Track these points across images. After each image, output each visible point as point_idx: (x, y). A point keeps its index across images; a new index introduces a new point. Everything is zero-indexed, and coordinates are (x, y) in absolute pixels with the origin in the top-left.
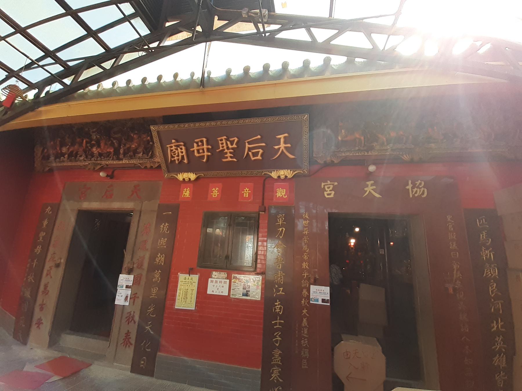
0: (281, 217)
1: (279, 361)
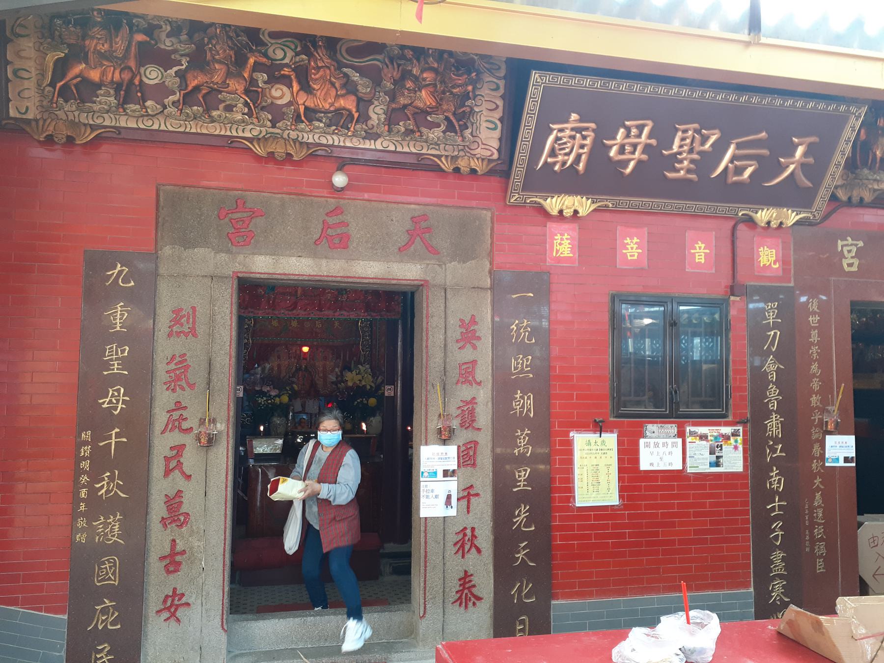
0: (771, 308)
1: (781, 569)
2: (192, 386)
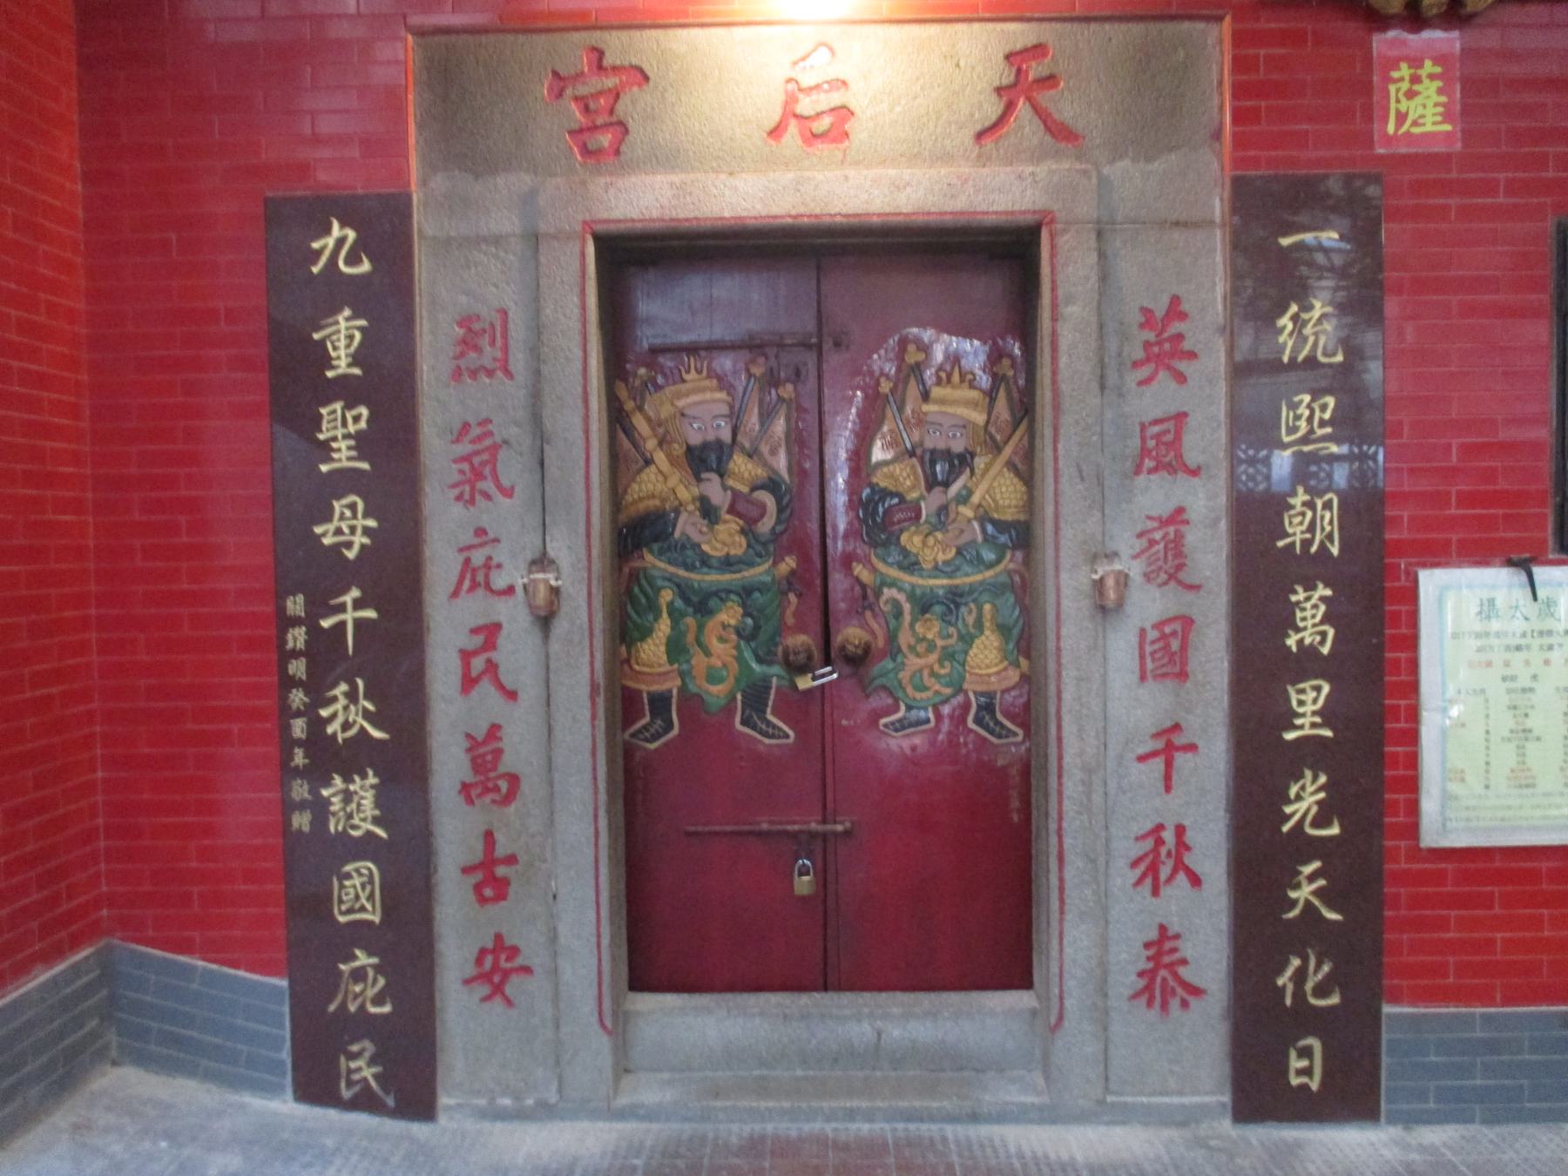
2: (508, 493)
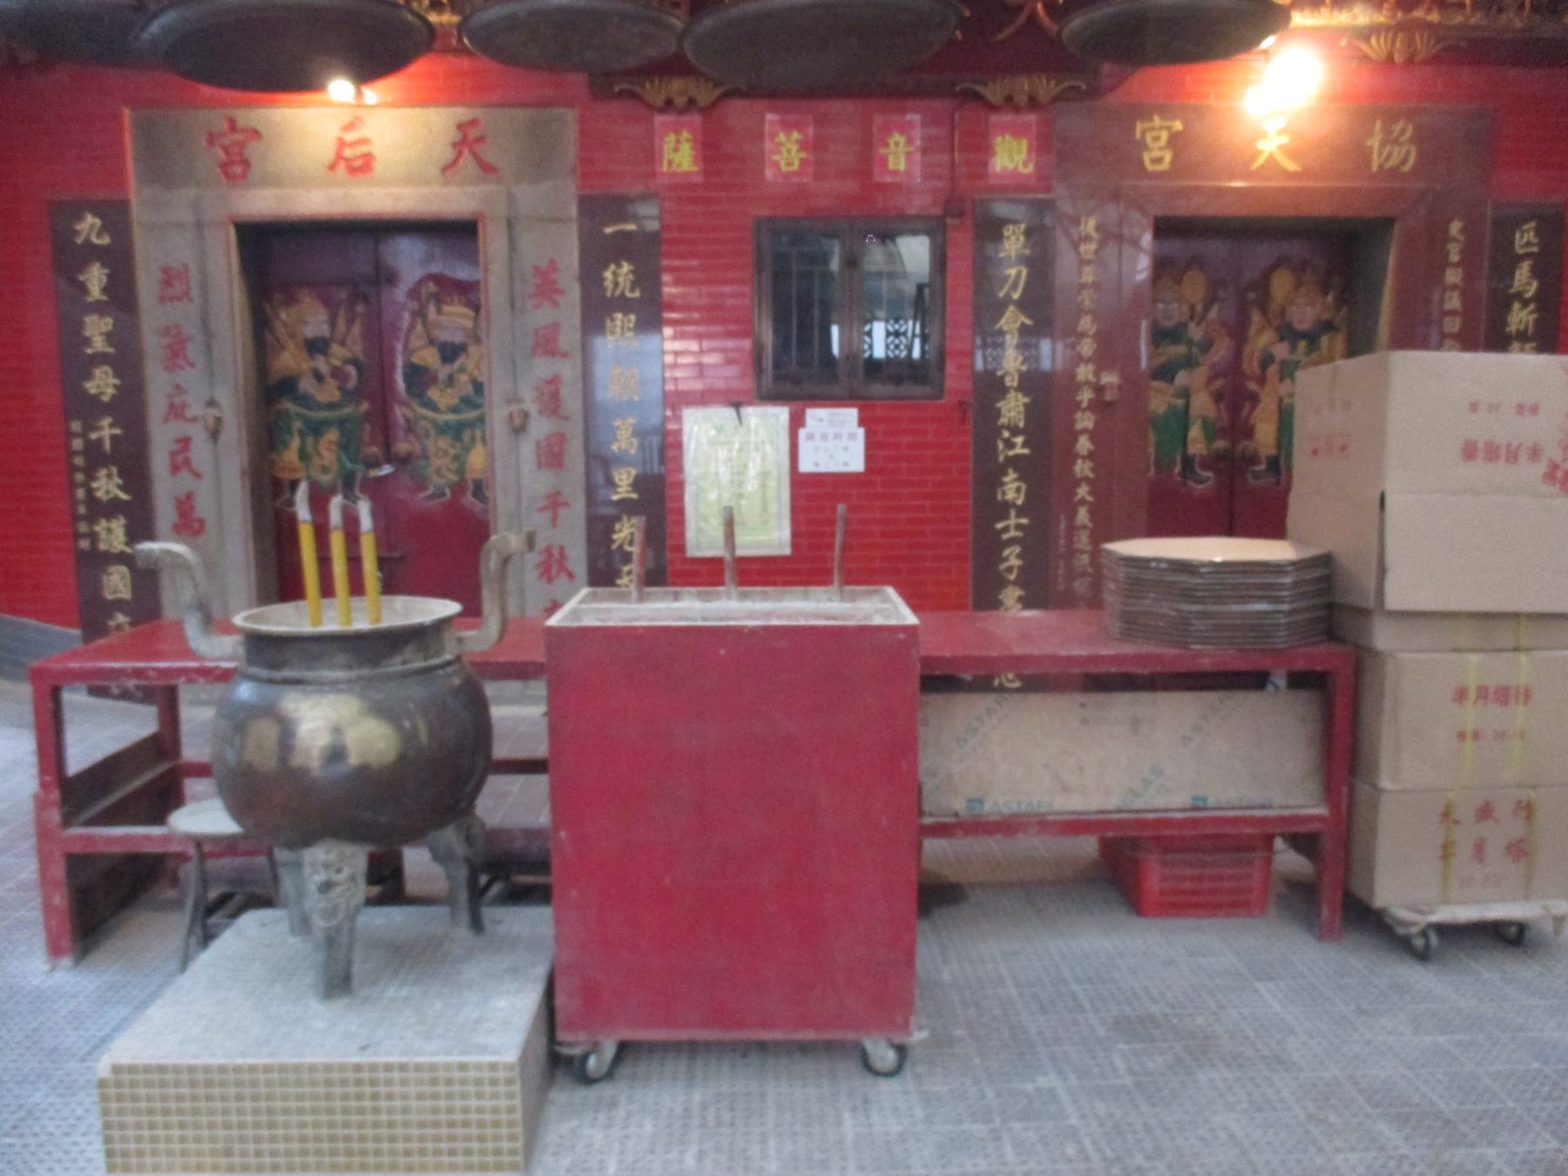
2: (192, 365)
